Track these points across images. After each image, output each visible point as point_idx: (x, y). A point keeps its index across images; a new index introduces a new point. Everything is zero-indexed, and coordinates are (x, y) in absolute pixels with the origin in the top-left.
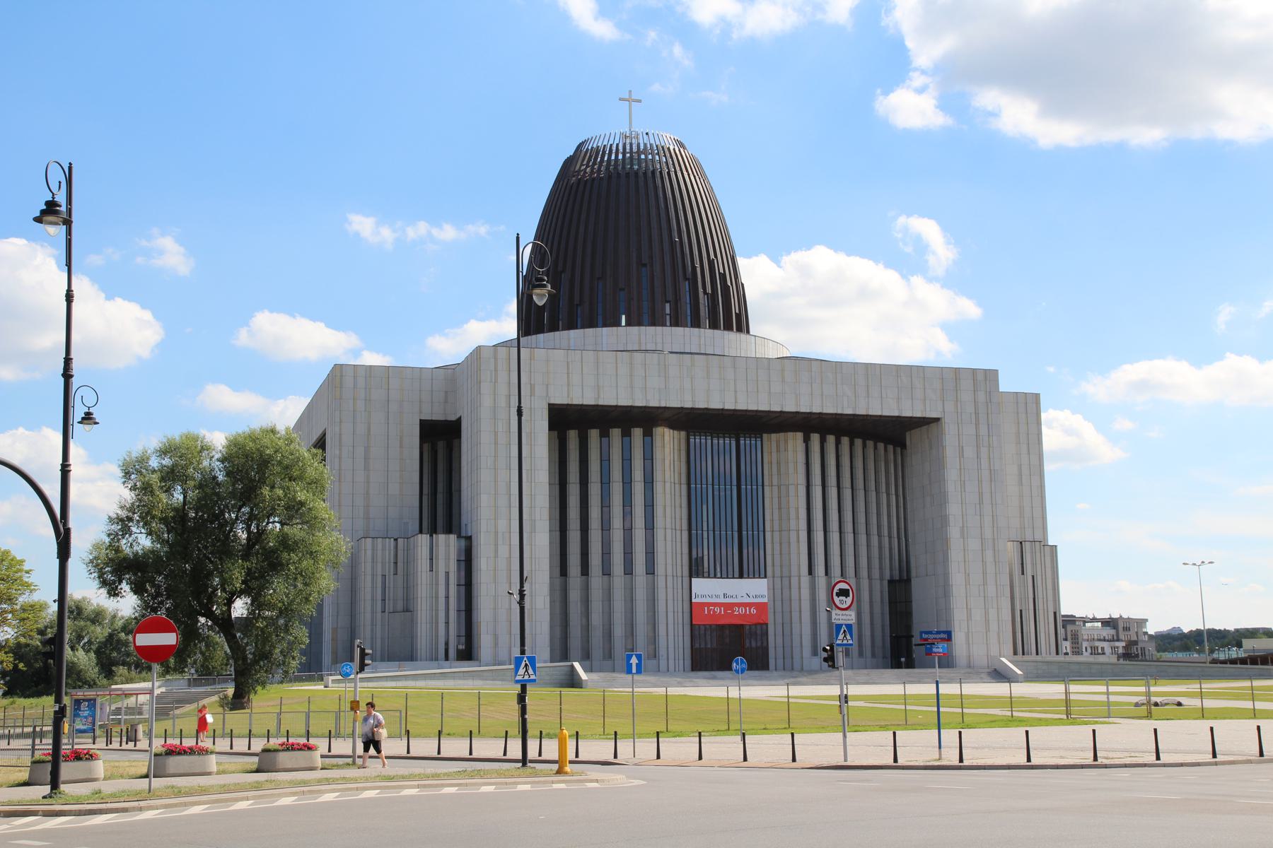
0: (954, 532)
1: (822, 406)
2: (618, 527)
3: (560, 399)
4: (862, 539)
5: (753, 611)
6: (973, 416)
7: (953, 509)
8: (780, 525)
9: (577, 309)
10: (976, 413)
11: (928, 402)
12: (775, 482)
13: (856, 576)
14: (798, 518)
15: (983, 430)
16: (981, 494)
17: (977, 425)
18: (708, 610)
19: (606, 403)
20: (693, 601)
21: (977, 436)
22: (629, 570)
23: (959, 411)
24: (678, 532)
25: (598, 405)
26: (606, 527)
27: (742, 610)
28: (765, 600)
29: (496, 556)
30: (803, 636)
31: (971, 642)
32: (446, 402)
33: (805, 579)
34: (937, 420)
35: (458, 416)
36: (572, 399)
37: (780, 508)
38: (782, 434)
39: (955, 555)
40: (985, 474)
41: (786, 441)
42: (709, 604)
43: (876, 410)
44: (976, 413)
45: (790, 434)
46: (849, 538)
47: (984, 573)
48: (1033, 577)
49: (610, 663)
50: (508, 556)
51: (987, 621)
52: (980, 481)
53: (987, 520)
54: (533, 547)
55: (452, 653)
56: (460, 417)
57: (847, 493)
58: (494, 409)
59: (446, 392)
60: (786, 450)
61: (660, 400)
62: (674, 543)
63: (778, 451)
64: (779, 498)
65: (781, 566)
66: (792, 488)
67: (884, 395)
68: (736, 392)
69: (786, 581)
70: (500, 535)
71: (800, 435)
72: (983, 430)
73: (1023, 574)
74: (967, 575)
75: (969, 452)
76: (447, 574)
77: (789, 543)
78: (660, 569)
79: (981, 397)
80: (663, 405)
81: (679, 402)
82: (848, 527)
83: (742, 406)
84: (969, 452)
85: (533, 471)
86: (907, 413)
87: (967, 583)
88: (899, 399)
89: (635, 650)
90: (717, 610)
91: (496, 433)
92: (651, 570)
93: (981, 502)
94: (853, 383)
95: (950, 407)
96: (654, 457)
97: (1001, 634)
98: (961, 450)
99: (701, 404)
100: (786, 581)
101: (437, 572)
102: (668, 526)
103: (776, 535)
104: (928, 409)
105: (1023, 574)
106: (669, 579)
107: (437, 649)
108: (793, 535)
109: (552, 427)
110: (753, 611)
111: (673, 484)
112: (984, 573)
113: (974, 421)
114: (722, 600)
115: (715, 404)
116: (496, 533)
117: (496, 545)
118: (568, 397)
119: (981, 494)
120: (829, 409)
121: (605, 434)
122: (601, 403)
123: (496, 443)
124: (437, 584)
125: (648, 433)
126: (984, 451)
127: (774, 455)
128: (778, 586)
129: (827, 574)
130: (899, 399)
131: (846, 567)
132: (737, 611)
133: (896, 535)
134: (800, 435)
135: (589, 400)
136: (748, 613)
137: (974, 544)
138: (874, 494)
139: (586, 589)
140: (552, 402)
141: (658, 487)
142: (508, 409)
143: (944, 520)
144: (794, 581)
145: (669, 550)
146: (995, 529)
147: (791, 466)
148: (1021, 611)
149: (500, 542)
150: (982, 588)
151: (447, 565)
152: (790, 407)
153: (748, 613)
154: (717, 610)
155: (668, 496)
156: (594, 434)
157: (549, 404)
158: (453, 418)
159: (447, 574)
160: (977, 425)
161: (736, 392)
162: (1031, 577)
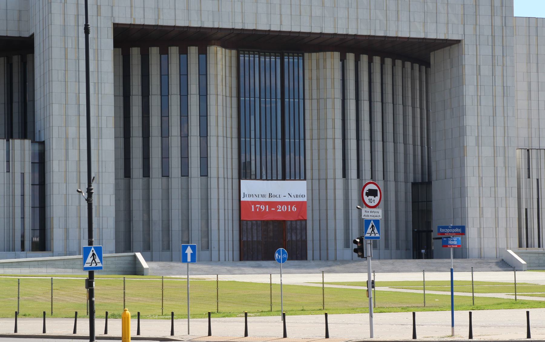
0: (470, 141)
1: (357, 29)
2: (176, 135)
3: (124, 19)
4: (390, 146)
5: (294, 209)
7: (470, 121)
8: (319, 134)
10: (493, 36)
11: (450, 25)
12: (315, 96)
13: (384, 179)
14: (334, 128)
15: (498, 51)
16: (494, 108)
17: (493, 46)
18: (255, 208)
19: (165, 24)
20: (242, 199)
21: (493, 56)
22: (185, 173)
23: (478, 33)
24: (229, 140)
25: (157, 26)
26: (165, 134)
27: (284, 208)
28: (305, 199)
29: (67, 159)
30: (337, 231)
31: (482, 236)
32: (20, 20)
33: (340, 182)
34: (458, 42)
35: (31, 34)
36: (134, 19)
37: (318, 119)
38: (321, 54)
39: (471, 161)
40: (499, 89)
41: (325, 60)
42: (255, 203)
43: (404, 33)
44: (493, 36)
45: (329, 54)
46: (379, 146)
47: (496, 177)
48: (538, 180)
49: (168, 253)
50: (77, 159)
51: (497, 218)
52: (494, 96)
53: (500, 131)
54: (100, 151)
55: (28, 244)
56: (33, 35)
57: (378, 107)
58: (64, 27)
59: (20, 11)
60: (325, 67)
61: (213, 22)
62: (225, 149)
63: (318, 68)
64: (318, 110)
65: (319, 170)
66: (329, 102)
67: (412, 20)
68: (281, 15)
69: (323, 182)
70: (70, 141)
71: (337, 55)
72: (498, 51)
73: (529, 177)
74: (481, 179)
75: (486, 70)
76: (23, 175)
77: (326, 149)
78: (213, 172)
79: (498, 21)
80: (216, 26)
81: (231, 24)
82: (378, 136)
83: (286, 28)
84: (486, 70)
85: (100, 84)
86: (432, 35)
87: (480, 185)
88: (425, 23)
89: (190, 242)
90: (263, 208)
91: (66, 49)
92: (205, 172)
93: (494, 115)
94: (385, 9)
95: (469, 30)
96: (208, 73)
97: (508, 229)
98: (479, 68)
99: (250, 26)
100: (323, 182)
101: (14, 173)
102: (220, 133)
103: (315, 142)
104: (450, 32)
105: (529, 177)
106: (221, 181)
107: (14, 241)
108: (330, 143)
109: (117, 44)
110: (294, 209)
111: (224, 97)
112: (496, 177)
113: (490, 43)
115: (263, 26)
116: (67, 139)
117: (67, 150)
118: (131, 17)
119: (494, 108)
120: (364, 31)
121: (164, 52)
122: (161, 23)
123: (66, 58)
124: (14, 184)
125: (203, 52)
126: (498, 69)
127: (314, 72)
128: (316, 187)
129: (358, 176)
130: (425, 23)
131: (375, 171)
132: (280, 209)
133: (419, 143)
134: (337, 55)
135: (150, 20)
136: (289, 210)
137: (487, 151)
138: (401, 107)
139: (147, 189)
140: (117, 22)
141: (212, 100)
142: (76, 27)
143: (462, 131)
144: (330, 183)
145: (221, 155)
146: (506, 138)
147: (329, 82)
148: (526, 209)
149: (70, 147)
150: (493, 189)
151: (23, 167)
152: (329, 29)
153: (289, 210)
154: (263, 208)
155: (220, 108)
156: (154, 51)
157: (114, 24)
158: (26, 35)
159: (23, 175)
160: (493, 46)
161: (281, 15)
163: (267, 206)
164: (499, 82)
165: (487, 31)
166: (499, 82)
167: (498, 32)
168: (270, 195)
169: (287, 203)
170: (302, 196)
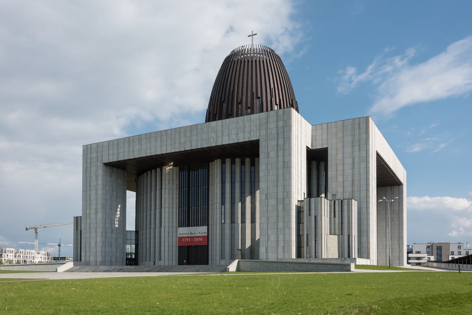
5: (201, 239)
6: (276, 135)
9: (230, 116)
15: (281, 141)
16: (277, 175)
18: (184, 240)
27: (197, 239)
40: (281, 164)
42: (184, 237)
44: (277, 133)
51: (278, 241)
53: (280, 189)
67: (230, 133)
73: (310, 215)
75: (273, 154)
79: (281, 124)
84: (273, 154)
90: (187, 240)
95: (263, 132)
104: (252, 136)
110: (201, 239)
113: (276, 138)
114: (190, 235)
119: (277, 175)
126: (281, 153)
130: (237, 134)
154: (187, 240)
162: (314, 216)
163: (190, 239)
164: (281, 159)
165: (274, 131)
166: (281, 159)
167: (280, 130)
168: (191, 233)
169: (198, 237)
170: (205, 233)
